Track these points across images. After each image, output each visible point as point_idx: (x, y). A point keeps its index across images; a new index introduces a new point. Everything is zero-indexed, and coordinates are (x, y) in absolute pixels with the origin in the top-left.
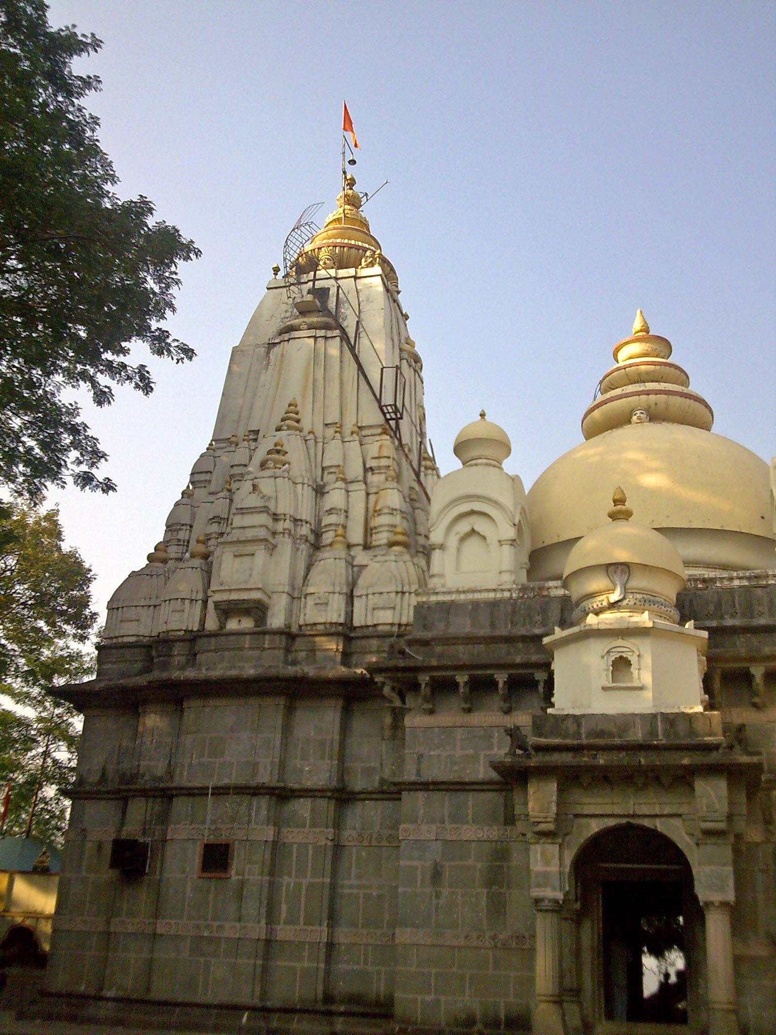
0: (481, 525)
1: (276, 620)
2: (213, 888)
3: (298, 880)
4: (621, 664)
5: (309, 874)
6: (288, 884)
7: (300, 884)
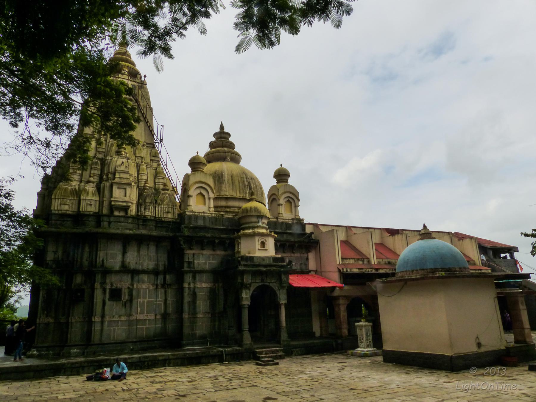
2: (115, 304)
3: (144, 300)
4: (263, 244)
5: (147, 298)
6: (140, 302)
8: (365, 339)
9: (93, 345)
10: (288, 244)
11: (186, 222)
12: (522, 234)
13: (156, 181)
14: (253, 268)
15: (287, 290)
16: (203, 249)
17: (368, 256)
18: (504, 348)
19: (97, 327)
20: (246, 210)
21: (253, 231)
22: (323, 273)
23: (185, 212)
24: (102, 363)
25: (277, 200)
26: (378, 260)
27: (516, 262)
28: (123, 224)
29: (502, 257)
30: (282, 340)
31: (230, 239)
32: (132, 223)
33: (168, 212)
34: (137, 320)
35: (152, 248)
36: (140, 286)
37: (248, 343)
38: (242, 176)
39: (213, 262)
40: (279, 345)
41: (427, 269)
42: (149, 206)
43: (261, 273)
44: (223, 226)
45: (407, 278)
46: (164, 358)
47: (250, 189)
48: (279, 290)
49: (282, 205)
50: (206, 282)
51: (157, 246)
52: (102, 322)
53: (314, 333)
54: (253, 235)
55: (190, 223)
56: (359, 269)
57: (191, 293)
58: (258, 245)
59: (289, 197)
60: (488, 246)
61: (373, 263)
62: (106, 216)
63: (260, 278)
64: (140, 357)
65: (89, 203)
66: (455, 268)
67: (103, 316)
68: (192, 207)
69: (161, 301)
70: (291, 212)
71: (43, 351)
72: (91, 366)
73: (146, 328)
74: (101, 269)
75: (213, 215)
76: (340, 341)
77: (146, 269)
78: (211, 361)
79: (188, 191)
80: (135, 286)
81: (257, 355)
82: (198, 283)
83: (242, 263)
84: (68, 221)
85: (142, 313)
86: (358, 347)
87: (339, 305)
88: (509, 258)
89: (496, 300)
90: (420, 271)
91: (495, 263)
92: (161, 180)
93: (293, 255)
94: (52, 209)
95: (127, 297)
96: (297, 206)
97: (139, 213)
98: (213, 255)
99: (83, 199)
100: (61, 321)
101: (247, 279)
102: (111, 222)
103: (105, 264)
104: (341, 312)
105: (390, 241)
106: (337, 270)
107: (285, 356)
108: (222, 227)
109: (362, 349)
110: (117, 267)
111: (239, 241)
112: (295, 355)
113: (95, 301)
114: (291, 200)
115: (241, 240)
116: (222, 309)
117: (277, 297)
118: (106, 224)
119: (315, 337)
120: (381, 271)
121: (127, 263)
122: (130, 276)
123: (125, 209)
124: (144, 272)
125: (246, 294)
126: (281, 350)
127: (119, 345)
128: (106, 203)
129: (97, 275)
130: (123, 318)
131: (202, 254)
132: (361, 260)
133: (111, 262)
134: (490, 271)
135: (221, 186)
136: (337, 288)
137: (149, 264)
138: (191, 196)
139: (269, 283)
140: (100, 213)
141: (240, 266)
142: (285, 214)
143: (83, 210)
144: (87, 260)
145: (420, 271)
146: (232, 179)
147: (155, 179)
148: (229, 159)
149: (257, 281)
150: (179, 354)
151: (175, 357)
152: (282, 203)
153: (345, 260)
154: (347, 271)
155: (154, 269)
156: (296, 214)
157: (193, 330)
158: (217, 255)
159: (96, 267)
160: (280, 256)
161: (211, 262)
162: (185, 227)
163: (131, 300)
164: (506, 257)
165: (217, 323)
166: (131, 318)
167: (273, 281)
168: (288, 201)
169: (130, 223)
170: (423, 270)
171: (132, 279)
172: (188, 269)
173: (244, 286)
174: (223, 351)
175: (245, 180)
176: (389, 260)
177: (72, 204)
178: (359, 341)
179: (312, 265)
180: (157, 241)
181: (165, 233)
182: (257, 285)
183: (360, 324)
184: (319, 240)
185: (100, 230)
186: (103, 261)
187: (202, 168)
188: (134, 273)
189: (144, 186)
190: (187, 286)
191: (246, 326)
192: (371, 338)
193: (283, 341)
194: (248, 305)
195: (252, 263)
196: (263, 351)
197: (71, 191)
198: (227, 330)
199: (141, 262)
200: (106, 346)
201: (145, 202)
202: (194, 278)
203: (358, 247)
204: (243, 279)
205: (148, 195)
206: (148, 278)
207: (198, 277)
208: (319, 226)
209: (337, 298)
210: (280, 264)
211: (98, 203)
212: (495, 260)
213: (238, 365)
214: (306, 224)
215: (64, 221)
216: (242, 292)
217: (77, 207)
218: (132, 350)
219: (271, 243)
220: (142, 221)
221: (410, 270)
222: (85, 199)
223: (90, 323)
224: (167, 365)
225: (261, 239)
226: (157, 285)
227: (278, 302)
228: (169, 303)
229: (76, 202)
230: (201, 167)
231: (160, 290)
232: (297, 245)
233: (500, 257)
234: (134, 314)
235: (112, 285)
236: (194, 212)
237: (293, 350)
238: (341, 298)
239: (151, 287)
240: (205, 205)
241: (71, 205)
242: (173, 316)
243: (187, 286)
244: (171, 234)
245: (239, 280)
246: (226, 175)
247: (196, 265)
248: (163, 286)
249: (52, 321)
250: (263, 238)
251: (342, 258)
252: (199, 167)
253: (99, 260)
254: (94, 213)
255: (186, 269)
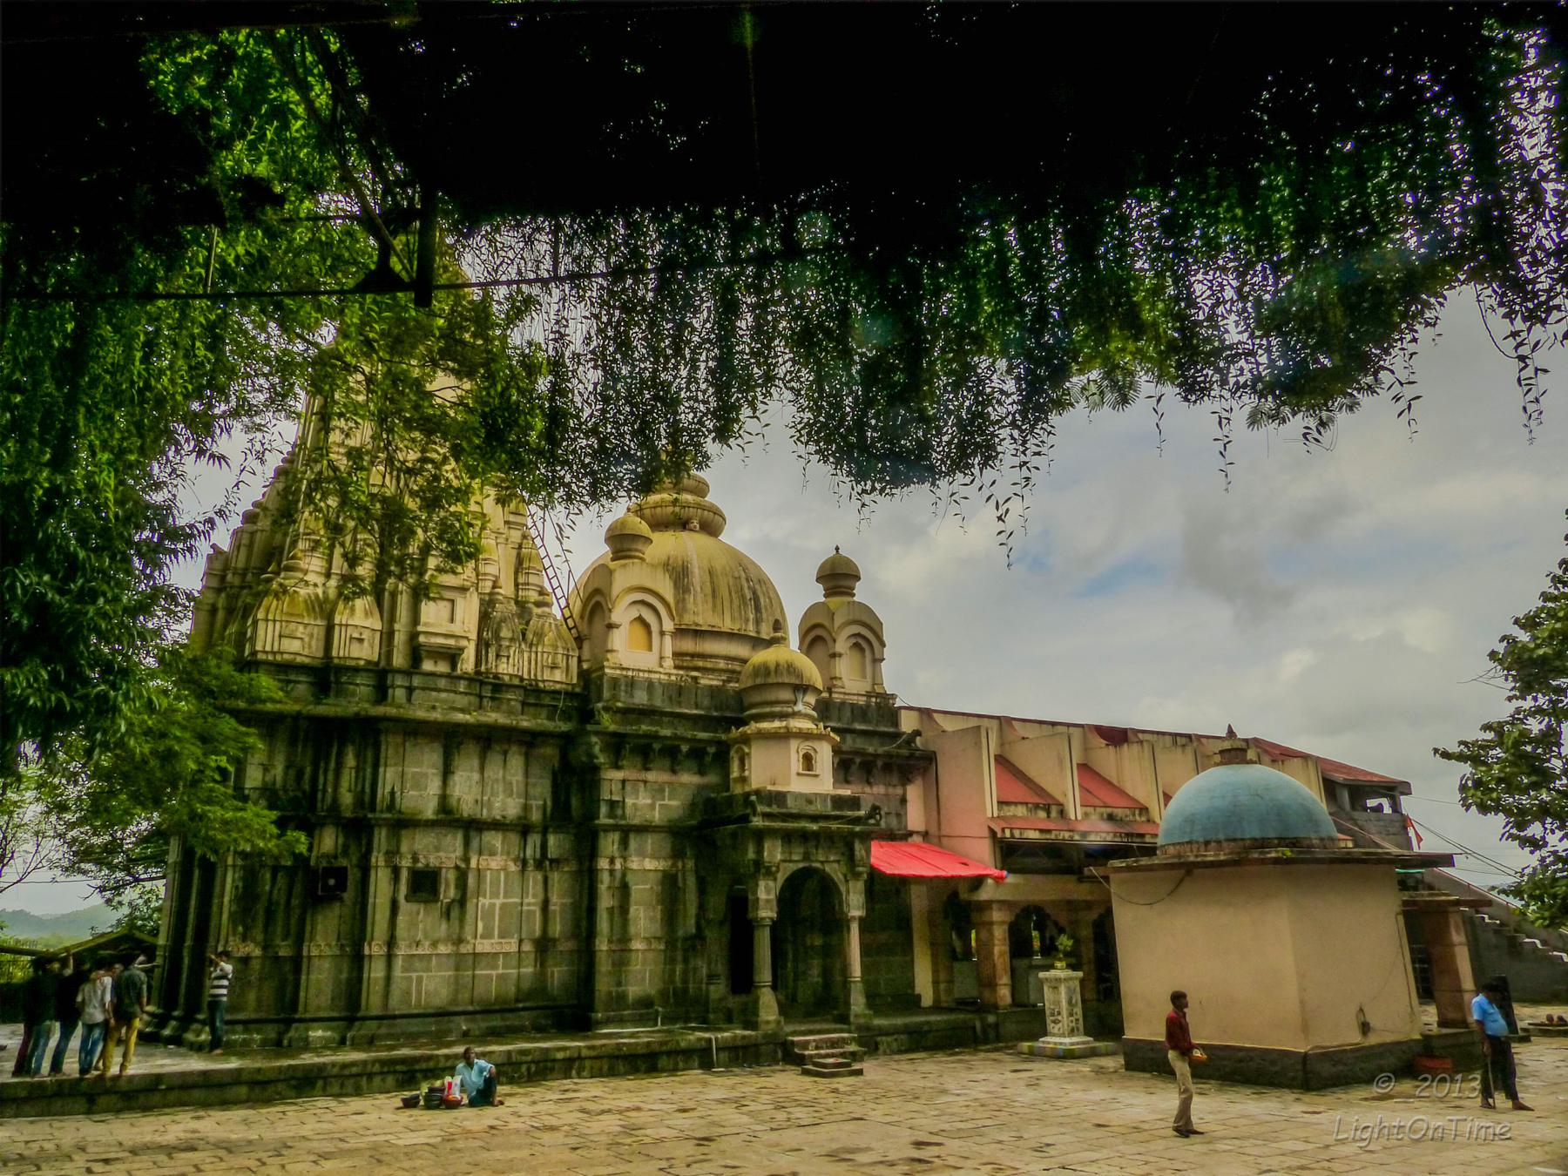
0: (649, 616)
1: (468, 664)
4: (808, 760)
6: (483, 906)
7: (494, 904)
8: (1065, 1013)
9: (364, 1019)
10: (858, 760)
11: (606, 694)
12: (1436, 751)
13: (521, 580)
14: (783, 821)
15: (866, 882)
16: (647, 769)
17: (1061, 799)
18: (1418, 1037)
19: (376, 971)
20: (763, 670)
21: (784, 724)
22: (944, 841)
23: (602, 668)
24: (417, 1067)
25: (830, 642)
26: (1085, 809)
27: (1405, 822)
28: (443, 695)
29: (1372, 809)
30: (852, 1013)
31: (719, 743)
32: (466, 694)
33: (554, 667)
34: (474, 954)
35: (516, 762)
36: (483, 864)
37: (772, 1018)
38: (736, 575)
39: (674, 803)
40: (845, 1027)
41: (1242, 840)
42: (509, 647)
43: (805, 836)
44: (697, 707)
45: (1192, 859)
46: (568, 1054)
47: (757, 609)
48: (847, 881)
49: (840, 655)
50: (653, 857)
51: (527, 756)
52: (390, 958)
53: (919, 997)
54: (785, 736)
55: (615, 698)
56: (1042, 831)
57: (617, 883)
58: (796, 764)
59: (858, 635)
60: (1339, 777)
61: (1073, 817)
62: (399, 671)
63: (802, 850)
64: (509, 1052)
65: (356, 635)
66: (1310, 839)
67: (391, 943)
68: (620, 655)
69: (534, 904)
70: (864, 677)
71: (234, 1033)
72: (388, 1072)
73: (498, 976)
74: (384, 816)
75: (673, 678)
76: (991, 1019)
77: (498, 817)
78: (681, 1065)
79: (610, 610)
80: (473, 864)
81: (796, 1050)
82: (635, 859)
83: (760, 808)
84: (298, 682)
85: (487, 935)
86: (1045, 1034)
87: (991, 923)
88: (1387, 810)
89: (1401, 919)
90: (1225, 844)
91: (1356, 825)
92: (532, 579)
93: (867, 789)
94: (259, 647)
95: (452, 893)
96: (878, 660)
97: (483, 668)
98: (670, 784)
99: (341, 625)
100: (280, 954)
101: (774, 852)
102: (416, 688)
103: (398, 800)
104: (996, 942)
105: (1107, 759)
106: (986, 833)
107: (865, 1053)
108: (695, 712)
109: (1059, 1038)
110: (429, 811)
111: (747, 750)
112: (885, 1053)
113: (371, 900)
114: (864, 645)
115: (750, 748)
116: (694, 931)
117: (841, 903)
118: (400, 694)
119: (920, 1007)
120: (1092, 837)
121: (453, 802)
122: (460, 836)
123: (453, 656)
124: (497, 825)
125: (768, 891)
126: (853, 1039)
127: (433, 1019)
128: (400, 638)
129: (376, 832)
130: (443, 949)
131: (645, 782)
132: (1043, 809)
133: (412, 796)
134: (1350, 844)
135: (684, 600)
136: (990, 881)
137: (507, 806)
138: (617, 626)
139: (822, 862)
140: (383, 664)
141: (754, 815)
142: (851, 682)
143: (341, 654)
144: (350, 791)
145: (1225, 844)
146: (712, 582)
147: (516, 573)
148: (695, 523)
149: (795, 857)
150: (604, 1045)
151: (593, 1053)
152: (842, 651)
153: (1005, 808)
154: (1012, 836)
155: (520, 818)
156: (876, 680)
157: (619, 984)
158: (682, 785)
159: (373, 809)
160: (846, 792)
161: (666, 802)
162: (607, 709)
163: (462, 902)
164: (1379, 808)
165: (679, 968)
166: (464, 949)
167: (832, 858)
168: (856, 645)
169: (461, 693)
170: (1234, 840)
171: (467, 844)
172: (611, 821)
173: (763, 871)
174: (710, 1040)
175: (745, 585)
176: (1109, 810)
177: (311, 636)
178: (1049, 1019)
179: (915, 817)
180: (529, 741)
181: (545, 722)
182: (793, 867)
183: (1053, 973)
184: (935, 753)
185: (380, 710)
186: (392, 793)
187: (640, 551)
188: (472, 827)
189: (491, 594)
190: (607, 867)
191: (764, 974)
192: (1078, 1010)
193: (856, 1016)
194: (771, 919)
195: (784, 811)
196: (810, 1038)
197: (306, 601)
198: (704, 986)
199: (485, 798)
200: (398, 1021)
201: (498, 638)
202: (624, 843)
203: (1033, 772)
204: (760, 851)
205: (503, 620)
206: (503, 842)
207: (633, 843)
208: (935, 715)
209: (987, 905)
210: (849, 813)
211: (378, 634)
212: (1356, 815)
213: (758, 1074)
214: (900, 708)
215: (289, 682)
216: (757, 885)
217: (322, 644)
218: (466, 1034)
219: (824, 756)
220: (490, 687)
221: (1201, 840)
222: (347, 625)
223: (358, 960)
224: (574, 1072)
225: (805, 747)
226: (524, 862)
227: (842, 912)
228: (555, 911)
229: (319, 633)
230: (640, 547)
231: (531, 874)
232: (880, 763)
233: (1365, 808)
234: (469, 938)
235: (415, 859)
236: (623, 669)
237: (879, 1039)
238: (995, 906)
239: (513, 867)
240: (650, 649)
241: (307, 639)
242: (566, 946)
243: (607, 867)
244: (564, 727)
245: (751, 855)
246: (696, 571)
247: (628, 812)
248: (539, 865)
249: (257, 952)
250: (808, 743)
251: (1000, 803)
252: (634, 546)
253: (383, 792)
254: (369, 662)
255: (603, 819)
